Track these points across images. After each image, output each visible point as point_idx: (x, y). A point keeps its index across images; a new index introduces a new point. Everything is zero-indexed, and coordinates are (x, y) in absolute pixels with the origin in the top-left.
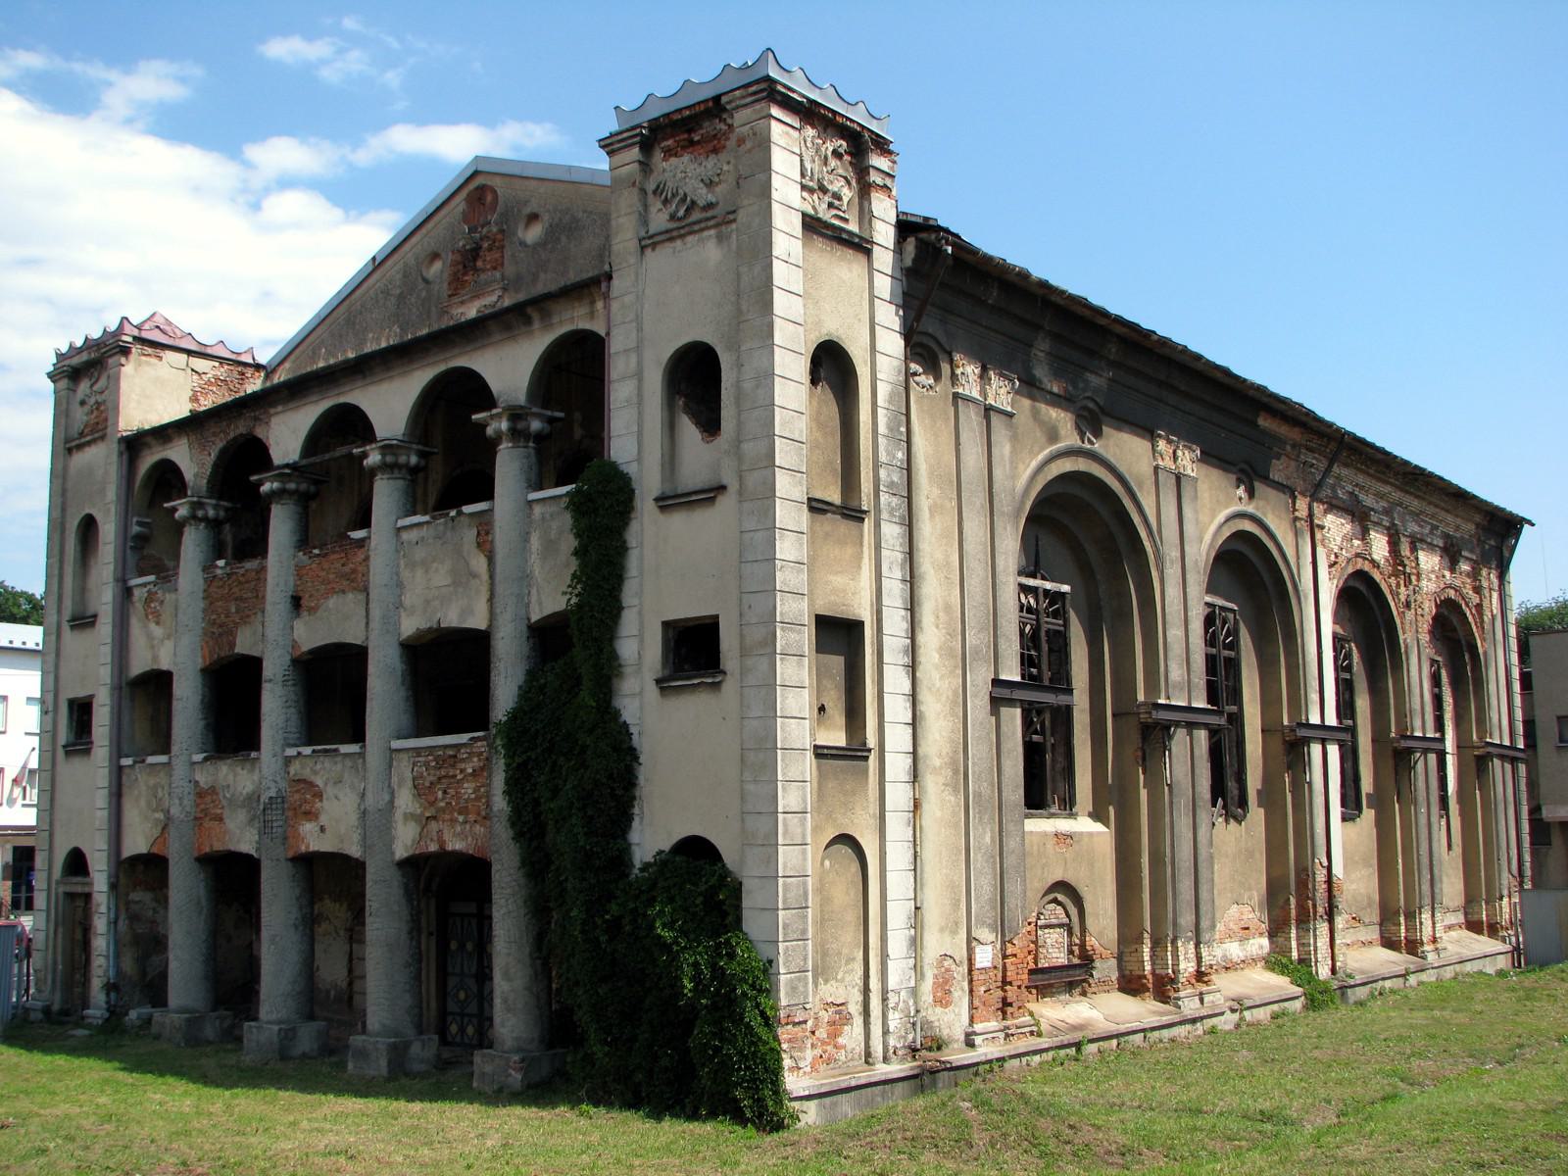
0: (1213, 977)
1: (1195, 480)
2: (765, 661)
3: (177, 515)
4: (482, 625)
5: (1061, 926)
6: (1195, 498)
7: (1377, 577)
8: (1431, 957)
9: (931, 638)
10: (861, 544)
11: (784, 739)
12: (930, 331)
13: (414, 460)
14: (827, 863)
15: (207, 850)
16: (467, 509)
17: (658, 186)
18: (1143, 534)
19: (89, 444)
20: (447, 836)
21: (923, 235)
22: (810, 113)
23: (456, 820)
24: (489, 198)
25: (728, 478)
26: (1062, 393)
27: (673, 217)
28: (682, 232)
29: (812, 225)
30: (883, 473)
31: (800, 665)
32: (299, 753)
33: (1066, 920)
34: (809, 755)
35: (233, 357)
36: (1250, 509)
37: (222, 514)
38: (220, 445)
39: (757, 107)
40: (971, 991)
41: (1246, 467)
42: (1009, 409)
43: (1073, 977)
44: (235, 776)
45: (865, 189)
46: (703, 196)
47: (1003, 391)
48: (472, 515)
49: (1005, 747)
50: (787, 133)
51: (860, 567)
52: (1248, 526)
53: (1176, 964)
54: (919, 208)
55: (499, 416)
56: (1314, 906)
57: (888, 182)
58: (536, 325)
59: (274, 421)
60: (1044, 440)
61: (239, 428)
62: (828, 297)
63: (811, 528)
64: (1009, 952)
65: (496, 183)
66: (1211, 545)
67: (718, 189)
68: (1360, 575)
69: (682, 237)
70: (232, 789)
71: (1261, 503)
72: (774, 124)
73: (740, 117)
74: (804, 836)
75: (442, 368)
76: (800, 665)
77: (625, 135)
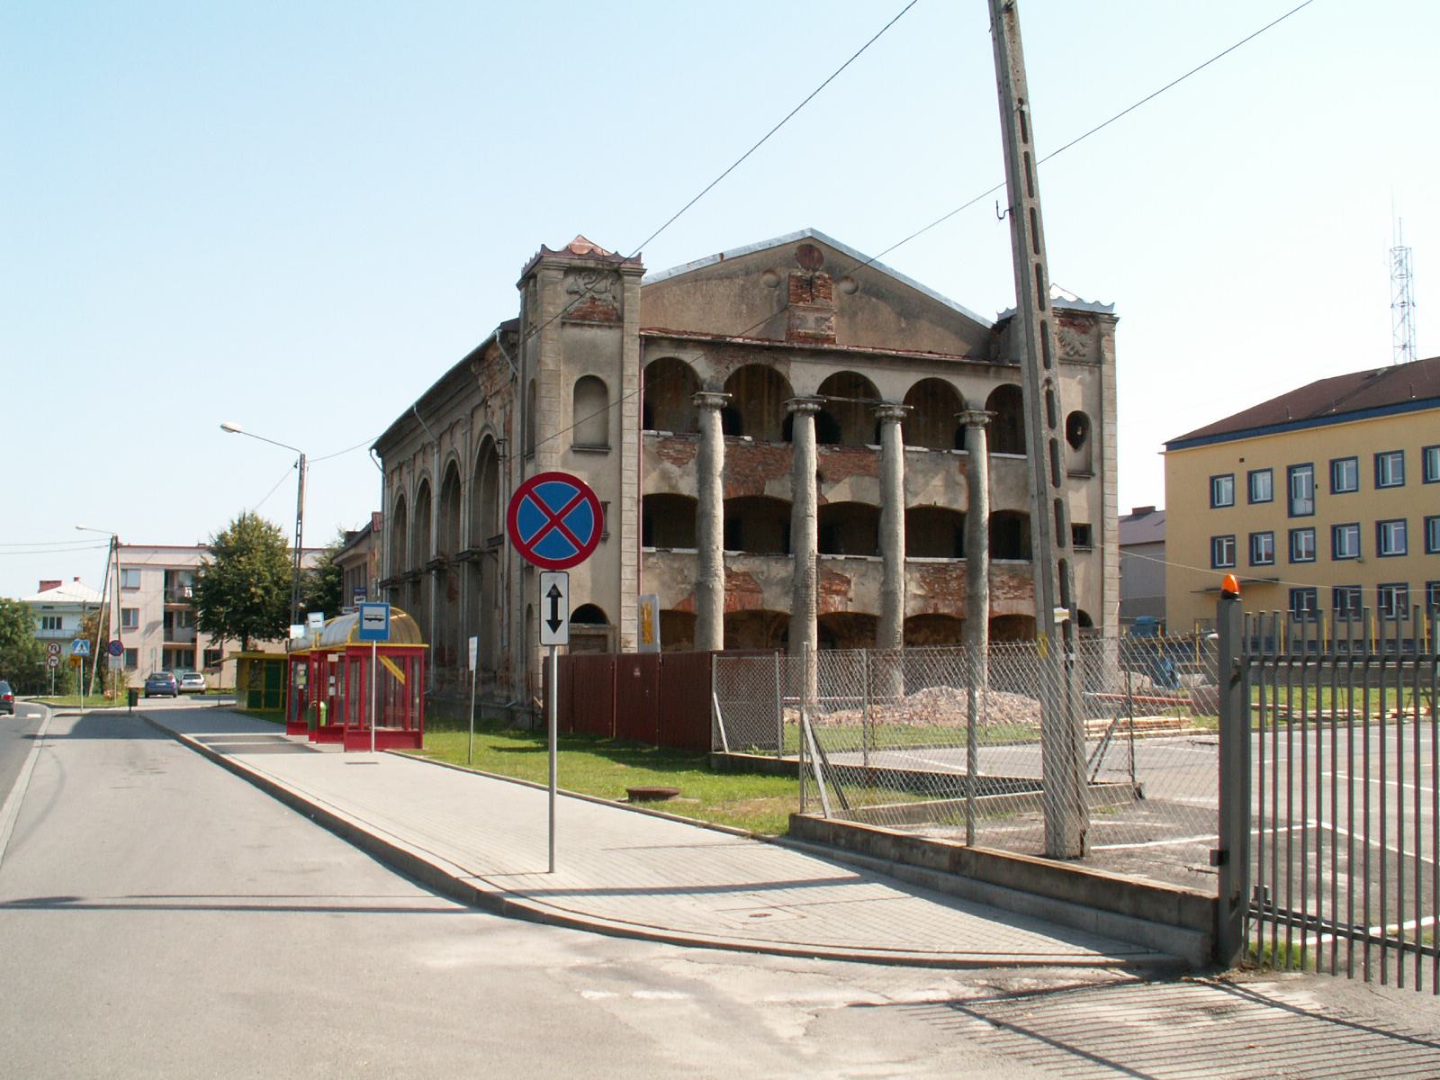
15: (739, 608)
16: (954, 451)
19: (591, 326)
20: (939, 606)
24: (816, 254)
32: (833, 558)
38: (738, 366)
44: (768, 566)
48: (956, 455)
59: (793, 365)
65: (824, 251)
70: (766, 575)
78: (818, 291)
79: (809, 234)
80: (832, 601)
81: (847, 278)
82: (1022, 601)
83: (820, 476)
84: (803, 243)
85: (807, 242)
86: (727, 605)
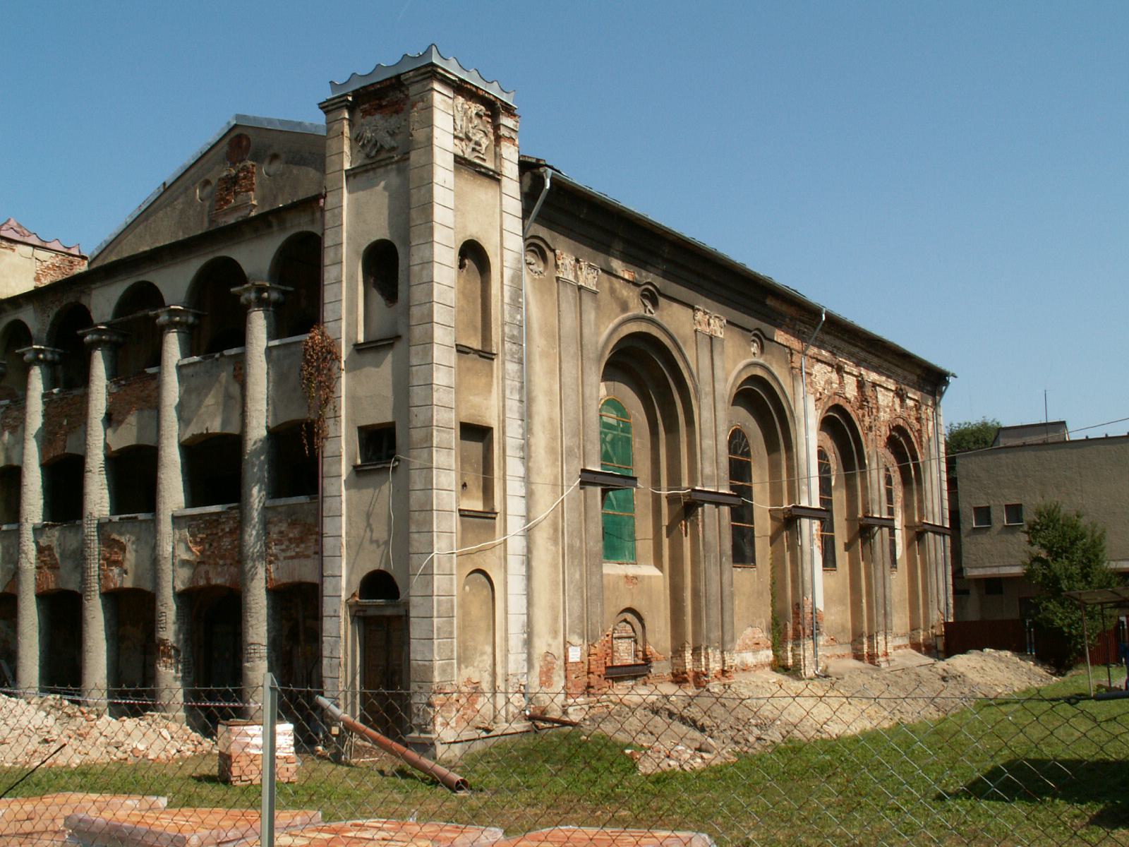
0: (735, 675)
1: (723, 340)
2: (425, 453)
3: (25, 358)
4: (237, 432)
5: (630, 638)
6: (722, 352)
7: (849, 409)
8: (883, 665)
9: (540, 441)
10: (492, 376)
11: (438, 504)
12: (541, 235)
13: (191, 319)
14: (467, 588)
15: (45, 588)
16: (227, 352)
17: (358, 135)
18: (686, 375)
20: (211, 575)
21: (536, 171)
22: (461, 88)
23: (218, 564)
24: (244, 143)
25: (402, 331)
26: (631, 279)
27: (368, 156)
28: (374, 166)
29: (460, 161)
30: (507, 329)
31: (449, 455)
33: (633, 634)
34: (456, 515)
35: (65, 250)
36: (761, 361)
37: (57, 357)
38: (56, 310)
39: (425, 83)
40: (566, 677)
41: (756, 332)
42: (594, 289)
43: (638, 671)
45: (498, 139)
46: (389, 142)
47: (590, 276)
48: (231, 356)
49: (591, 514)
50: (445, 101)
51: (490, 392)
52: (759, 372)
53: (707, 665)
54: (534, 154)
55: (248, 290)
56: (804, 629)
57: (513, 135)
58: (275, 228)
60: (618, 310)
61: (69, 299)
62: (470, 210)
63: (459, 366)
64: (593, 651)
65: (250, 133)
66: (734, 384)
67: (399, 137)
68: (837, 408)
69: (374, 169)
71: (769, 357)
72: (435, 94)
73: (413, 90)
74: (451, 569)
75: (211, 257)
76: (449, 455)
77: (336, 101)
78: (241, 186)
79: (235, 122)
80: (111, 574)
81: (275, 157)
82: (304, 561)
83: (110, 420)
84: (233, 134)
85: (237, 132)
86: (38, 586)
